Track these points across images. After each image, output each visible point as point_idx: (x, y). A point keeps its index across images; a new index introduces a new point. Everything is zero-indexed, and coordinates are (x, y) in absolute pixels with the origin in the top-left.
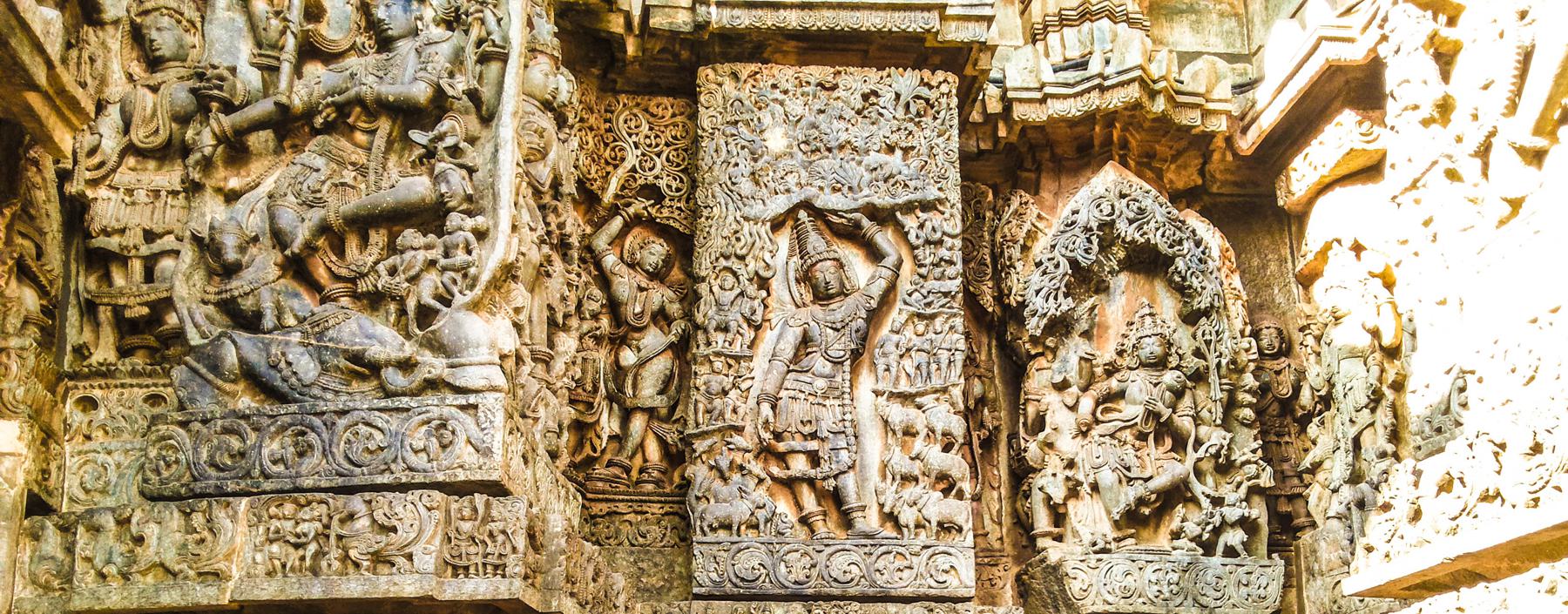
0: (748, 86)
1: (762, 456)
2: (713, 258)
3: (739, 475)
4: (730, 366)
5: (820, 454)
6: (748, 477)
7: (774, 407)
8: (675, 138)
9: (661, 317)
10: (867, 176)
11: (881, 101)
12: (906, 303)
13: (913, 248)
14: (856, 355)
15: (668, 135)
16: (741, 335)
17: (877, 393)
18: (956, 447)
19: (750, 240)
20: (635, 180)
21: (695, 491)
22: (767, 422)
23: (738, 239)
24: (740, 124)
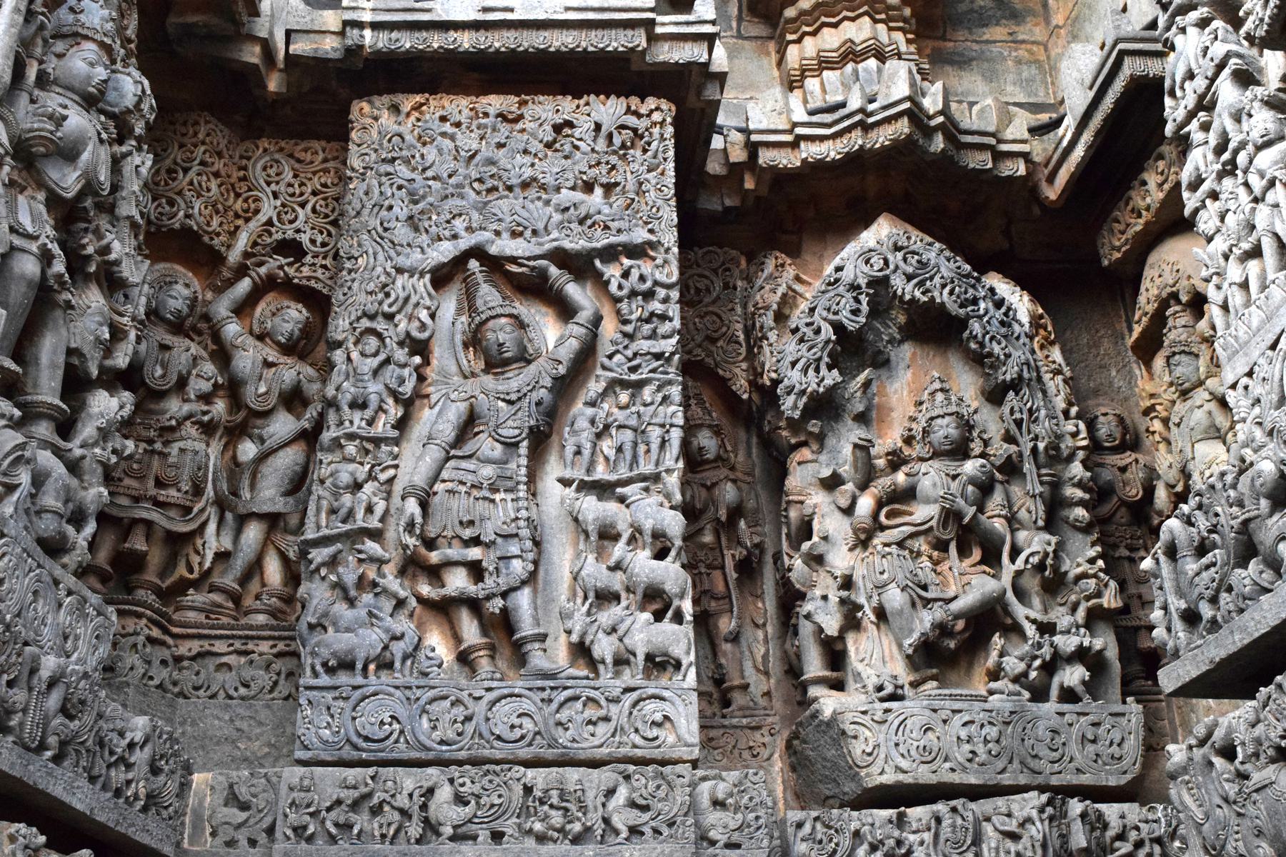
0: (412, 119)
1: (410, 571)
2: (353, 318)
3: (371, 595)
4: (367, 452)
5: (484, 564)
6: (383, 598)
7: (424, 505)
8: (325, 185)
10: (557, 217)
11: (577, 133)
12: (604, 368)
15: (316, 183)
16: (385, 412)
18: (673, 553)
19: (402, 295)
20: (270, 234)
23: (387, 295)
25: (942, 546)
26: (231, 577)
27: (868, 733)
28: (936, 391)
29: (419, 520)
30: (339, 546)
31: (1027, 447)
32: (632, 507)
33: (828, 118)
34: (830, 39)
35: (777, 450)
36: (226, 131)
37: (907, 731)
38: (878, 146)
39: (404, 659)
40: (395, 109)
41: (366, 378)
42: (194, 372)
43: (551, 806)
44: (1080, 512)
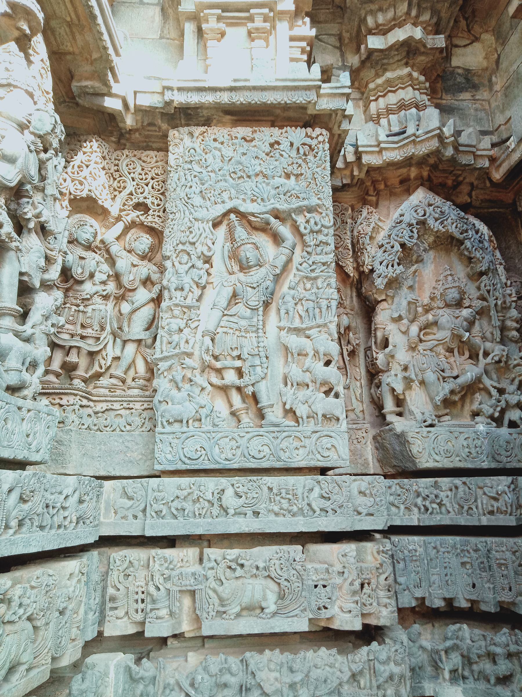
2: (175, 244)
3: (189, 385)
4: (185, 313)
6: (194, 387)
8: (157, 174)
9: (147, 282)
10: (273, 192)
11: (281, 147)
13: (302, 235)
14: (267, 304)
15: (152, 174)
17: (281, 329)
18: (333, 363)
19: (199, 233)
20: (132, 200)
21: (158, 397)
22: (208, 350)
24: (193, 162)
25: (450, 350)
26: (121, 371)
27: (419, 442)
28: (448, 275)
29: (211, 347)
30: (173, 361)
31: (492, 303)
32: (314, 340)
33: (396, 139)
34: (392, 99)
35: (369, 301)
36: (107, 145)
37: (439, 442)
38: (421, 153)
39: (206, 417)
40: (191, 134)
41: (182, 275)
42: (98, 269)
43: (282, 498)
44: (515, 333)
